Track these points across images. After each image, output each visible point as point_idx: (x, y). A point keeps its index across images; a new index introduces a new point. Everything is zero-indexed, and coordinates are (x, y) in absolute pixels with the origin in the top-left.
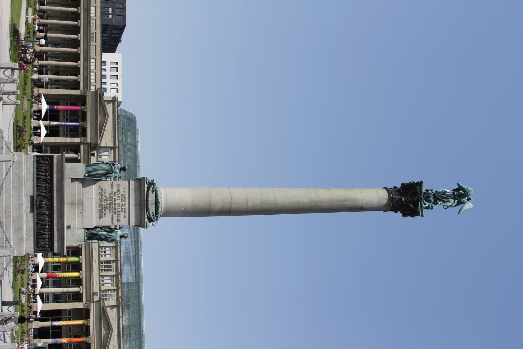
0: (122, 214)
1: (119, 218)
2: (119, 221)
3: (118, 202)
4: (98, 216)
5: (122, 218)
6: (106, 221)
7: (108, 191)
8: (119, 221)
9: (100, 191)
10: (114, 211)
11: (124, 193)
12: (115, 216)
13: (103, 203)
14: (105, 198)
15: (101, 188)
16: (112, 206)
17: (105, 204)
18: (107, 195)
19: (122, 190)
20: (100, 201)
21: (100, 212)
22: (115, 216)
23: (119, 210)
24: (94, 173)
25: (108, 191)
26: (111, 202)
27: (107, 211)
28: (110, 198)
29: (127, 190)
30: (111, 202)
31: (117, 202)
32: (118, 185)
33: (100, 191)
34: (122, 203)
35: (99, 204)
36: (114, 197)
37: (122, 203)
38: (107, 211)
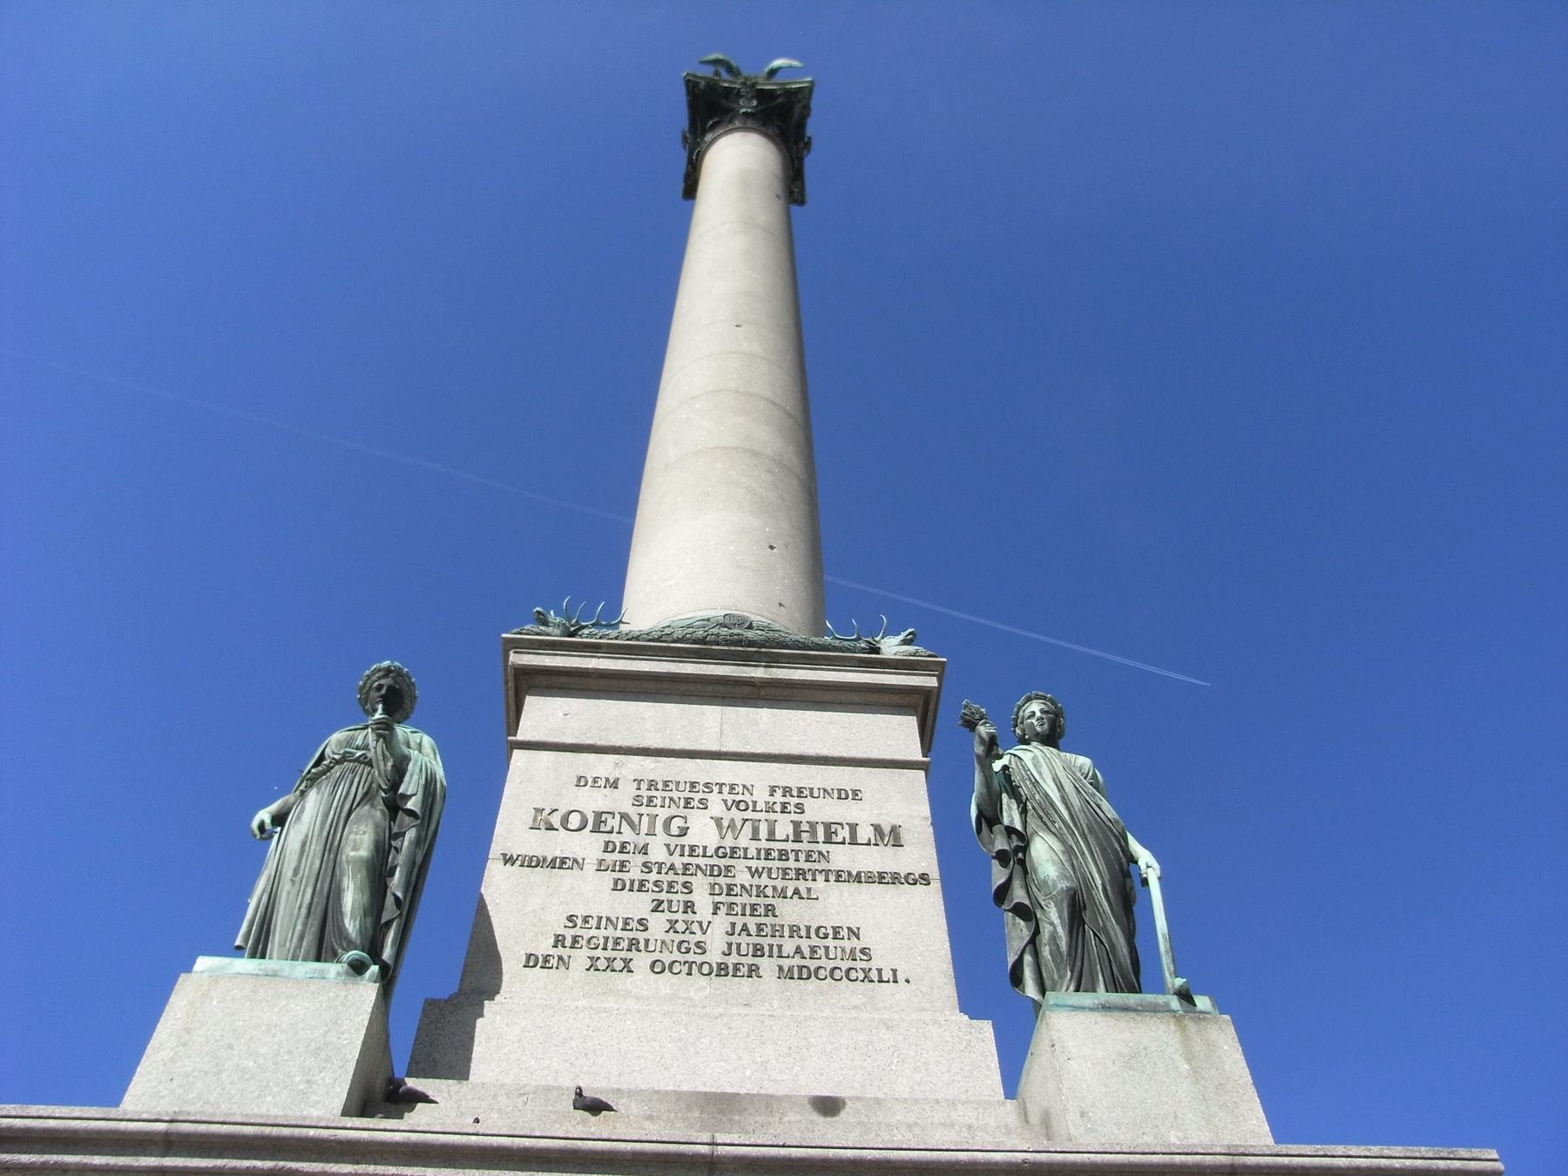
0: (818, 810)
1: (865, 833)
2: (891, 837)
3: (702, 831)
4: (851, 993)
5: (863, 815)
6: (910, 927)
7: (591, 893)
8: (891, 837)
9: (580, 957)
10: (805, 854)
11: (627, 790)
12: (841, 857)
13: (716, 942)
14: (658, 923)
15: (544, 947)
16: (743, 878)
17: (721, 923)
18: (637, 905)
19: (592, 801)
20: (685, 959)
21: (805, 974)
22: (841, 857)
23: (784, 828)
24: (352, 897)
25: (591, 893)
26: (700, 883)
27: (790, 912)
28: (667, 888)
29: (603, 766)
30: (700, 883)
31: (702, 831)
32: (543, 822)
33: (580, 957)
34: (716, 806)
35: (722, 970)
36: (658, 853)
37: (716, 806)
38: (790, 912)
